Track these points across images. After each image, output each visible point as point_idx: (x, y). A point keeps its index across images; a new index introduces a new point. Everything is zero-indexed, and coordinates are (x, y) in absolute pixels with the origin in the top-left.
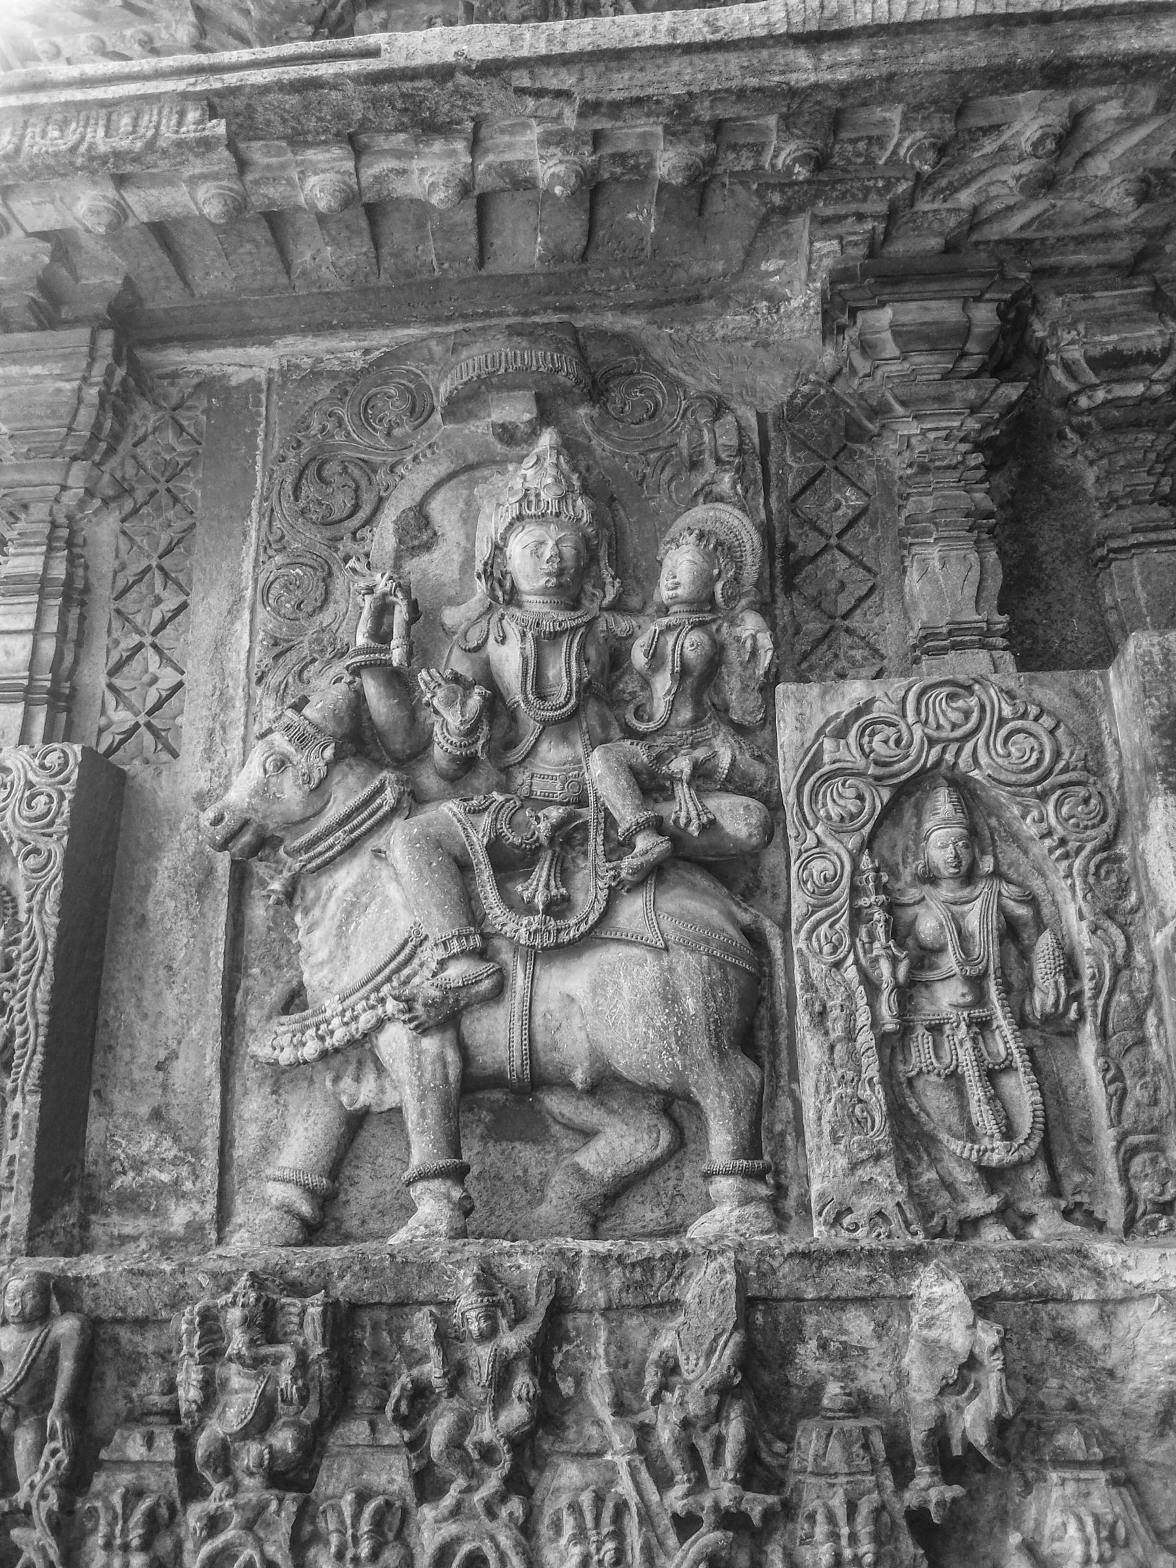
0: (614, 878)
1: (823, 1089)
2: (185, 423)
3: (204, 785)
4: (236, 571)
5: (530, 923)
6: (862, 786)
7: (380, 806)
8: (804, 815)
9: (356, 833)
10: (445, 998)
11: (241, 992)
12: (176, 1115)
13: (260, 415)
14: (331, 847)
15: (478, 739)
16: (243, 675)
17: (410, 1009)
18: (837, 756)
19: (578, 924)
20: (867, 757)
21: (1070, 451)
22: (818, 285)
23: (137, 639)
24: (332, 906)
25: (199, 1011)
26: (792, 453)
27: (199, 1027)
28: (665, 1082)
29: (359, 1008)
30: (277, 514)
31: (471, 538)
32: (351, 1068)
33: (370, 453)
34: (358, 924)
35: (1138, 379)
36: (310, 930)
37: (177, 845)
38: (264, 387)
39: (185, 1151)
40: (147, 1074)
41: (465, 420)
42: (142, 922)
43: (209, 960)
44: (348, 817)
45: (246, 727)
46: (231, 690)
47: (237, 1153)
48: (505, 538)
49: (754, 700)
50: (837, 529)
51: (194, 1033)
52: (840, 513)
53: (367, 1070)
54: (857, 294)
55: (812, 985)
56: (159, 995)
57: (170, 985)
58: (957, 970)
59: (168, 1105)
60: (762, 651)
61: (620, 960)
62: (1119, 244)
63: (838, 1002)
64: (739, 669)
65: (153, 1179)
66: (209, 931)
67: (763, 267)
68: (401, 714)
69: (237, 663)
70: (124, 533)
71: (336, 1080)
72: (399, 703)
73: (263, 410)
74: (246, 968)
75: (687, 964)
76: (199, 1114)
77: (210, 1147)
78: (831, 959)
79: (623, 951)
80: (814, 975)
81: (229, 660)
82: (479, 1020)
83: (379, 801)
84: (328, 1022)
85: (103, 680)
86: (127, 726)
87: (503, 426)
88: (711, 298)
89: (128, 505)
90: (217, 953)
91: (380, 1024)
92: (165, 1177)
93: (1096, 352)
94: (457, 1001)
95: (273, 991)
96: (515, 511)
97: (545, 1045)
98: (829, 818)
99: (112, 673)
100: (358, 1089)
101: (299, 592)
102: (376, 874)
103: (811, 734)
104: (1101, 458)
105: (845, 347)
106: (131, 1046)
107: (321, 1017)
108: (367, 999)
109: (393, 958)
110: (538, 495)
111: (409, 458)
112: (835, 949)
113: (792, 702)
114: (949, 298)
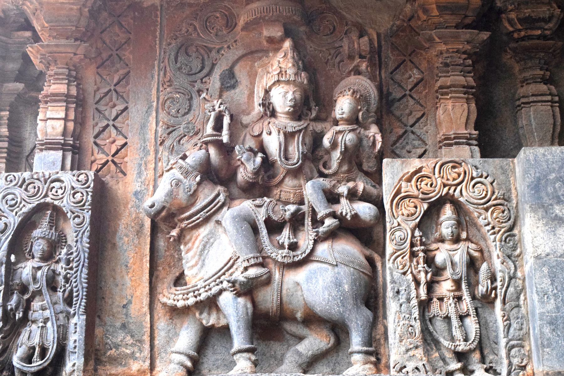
1: (397, 321)
4: (149, 94)
13: (157, 21)
19: (302, 254)
26: (392, 52)
28: (336, 317)
30: (168, 69)
33: (208, 43)
38: (159, 8)
50: (410, 87)
61: (318, 269)
63: (404, 288)
69: (151, 136)
70: (98, 73)
73: (159, 19)
78: (402, 271)
79: (319, 265)
80: (395, 277)
96: (276, 79)
101: (178, 105)
110: (286, 72)
111: (226, 46)
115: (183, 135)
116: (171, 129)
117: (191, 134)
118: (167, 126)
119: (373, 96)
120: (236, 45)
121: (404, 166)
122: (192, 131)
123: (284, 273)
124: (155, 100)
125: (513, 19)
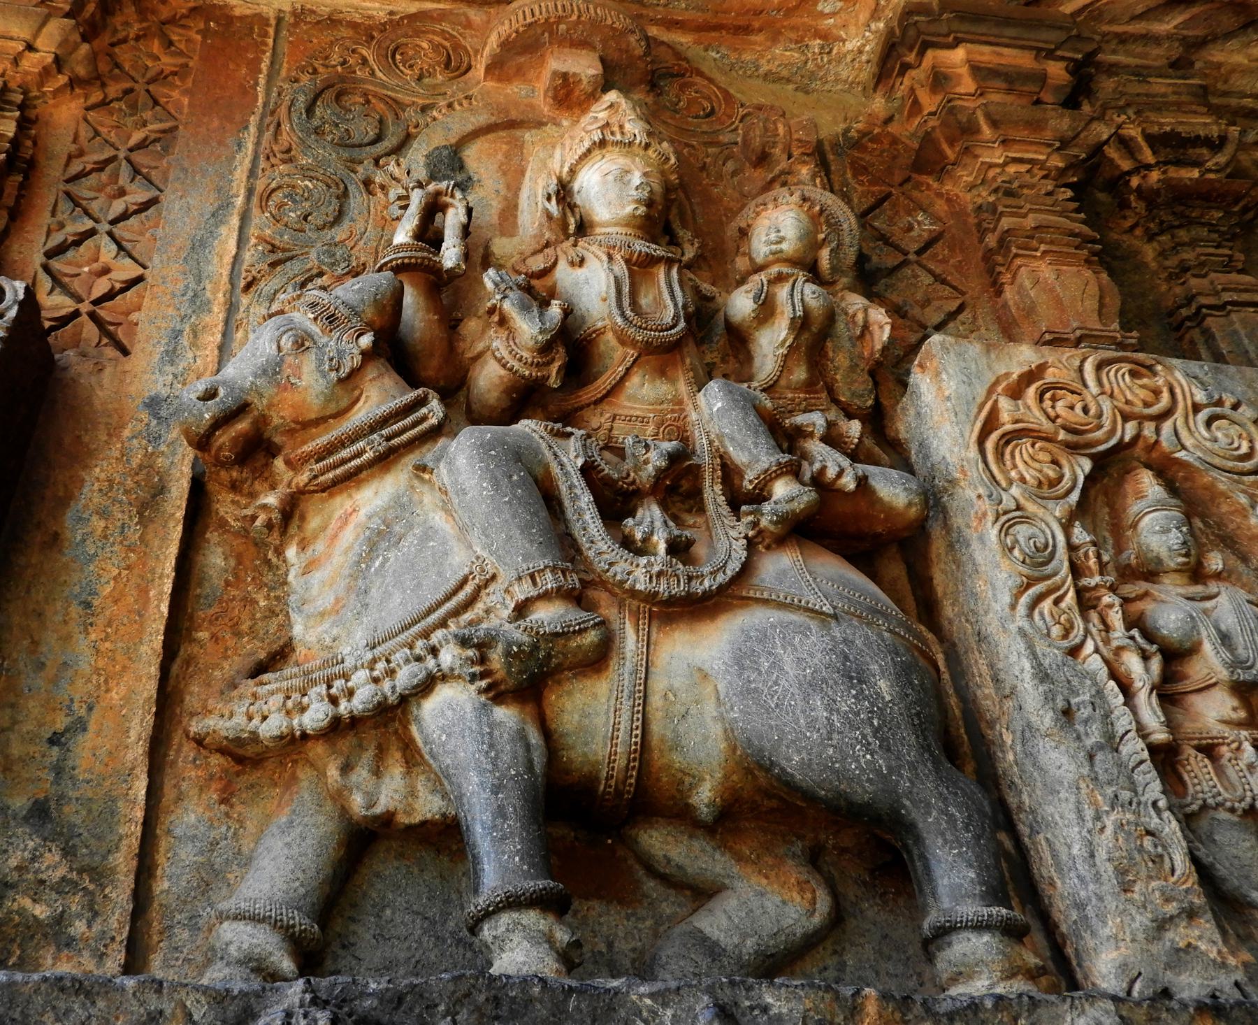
0: (755, 524)
1: (1089, 813)
2: (175, 38)
3: (164, 392)
4: (225, 177)
5: (650, 564)
6: (1055, 450)
7: (424, 418)
8: (994, 477)
9: (395, 442)
10: (535, 647)
11: (178, 661)
12: (73, 814)
13: (266, 45)
14: (358, 454)
15: (553, 360)
16: (225, 279)
17: (483, 660)
18: (1018, 415)
19: (713, 573)
20: (1053, 421)
21: (1127, 224)
22: (881, 25)
23: (89, 224)
24: (348, 535)
25: (124, 668)
26: (854, 176)
27: (123, 690)
28: (864, 791)
29: (398, 657)
30: (286, 127)
31: (514, 189)
32: (368, 756)
33: (397, 92)
34: (386, 560)
35: (1196, 164)
36: (306, 571)
37: (117, 454)
38: (273, 22)
39: (81, 872)
40: (32, 749)
41: (509, 80)
42: (55, 541)
43: (148, 600)
44: (384, 421)
45: (224, 335)
46: (208, 294)
47: (161, 885)
48: (573, 172)
49: (862, 383)
50: (915, 247)
51: (115, 696)
52: (913, 234)
53: (391, 761)
54: (932, 28)
55: (1047, 675)
56: (67, 639)
57: (86, 627)
58: (1224, 674)
59: (61, 797)
60: (875, 328)
61: (773, 627)
62: (1156, 51)
63: (1087, 697)
64: (848, 345)
65: (22, 912)
66: (152, 563)
67: (820, 7)
68: (438, 332)
69: (219, 267)
70: (86, 120)
71: (346, 769)
72: (440, 320)
73: (270, 41)
74: (189, 630)
75: (867, 638)
76: (109, 813)
77: (123, 868)
78: (1066, 644)
79: (774, 616)
80: (1047, 662)
81: (209, 262)
82: (570, 693)
83: (424, 410)
84: (346, 677)
85: (38, 258)
86: (63, 312)
87: (565, 76)
88: (760, 30)
89: (96, 97)
90: (161, 593)
91: (427, 686)
92: (41, 911)
93: (1155, 129)
94: (549, 656)
95: (226, 665)
96: (597, 136)
97: (663, 740)
98: (1023, 480)
99: (50, 254)
100: (377, 786)
101: (307, 204)
102: (416, 497)
103: (981, 392)
104: (1162, 232)
105: (899, 94)
106: (13, 706)
107: (337, 669)
108: (411, 647)
109: (448, 598)
110: (621, 127)
111: (443, 103)
112: (1066, 635)
113: (952, 355)
114: (1022, 47)
115: (315, 271)
116: (280, 255)
117: (340, 271)
118: (270, 247)
119: (845, 226)
120: (470, 104)
121: (993, 356)
122: (343, 265)
123: (654, 636)
124: (242, 191)
125: (1132, 139)
